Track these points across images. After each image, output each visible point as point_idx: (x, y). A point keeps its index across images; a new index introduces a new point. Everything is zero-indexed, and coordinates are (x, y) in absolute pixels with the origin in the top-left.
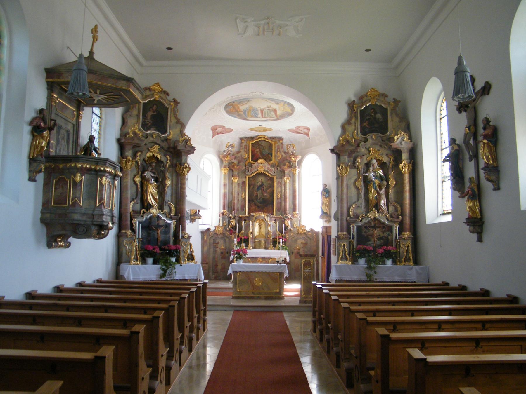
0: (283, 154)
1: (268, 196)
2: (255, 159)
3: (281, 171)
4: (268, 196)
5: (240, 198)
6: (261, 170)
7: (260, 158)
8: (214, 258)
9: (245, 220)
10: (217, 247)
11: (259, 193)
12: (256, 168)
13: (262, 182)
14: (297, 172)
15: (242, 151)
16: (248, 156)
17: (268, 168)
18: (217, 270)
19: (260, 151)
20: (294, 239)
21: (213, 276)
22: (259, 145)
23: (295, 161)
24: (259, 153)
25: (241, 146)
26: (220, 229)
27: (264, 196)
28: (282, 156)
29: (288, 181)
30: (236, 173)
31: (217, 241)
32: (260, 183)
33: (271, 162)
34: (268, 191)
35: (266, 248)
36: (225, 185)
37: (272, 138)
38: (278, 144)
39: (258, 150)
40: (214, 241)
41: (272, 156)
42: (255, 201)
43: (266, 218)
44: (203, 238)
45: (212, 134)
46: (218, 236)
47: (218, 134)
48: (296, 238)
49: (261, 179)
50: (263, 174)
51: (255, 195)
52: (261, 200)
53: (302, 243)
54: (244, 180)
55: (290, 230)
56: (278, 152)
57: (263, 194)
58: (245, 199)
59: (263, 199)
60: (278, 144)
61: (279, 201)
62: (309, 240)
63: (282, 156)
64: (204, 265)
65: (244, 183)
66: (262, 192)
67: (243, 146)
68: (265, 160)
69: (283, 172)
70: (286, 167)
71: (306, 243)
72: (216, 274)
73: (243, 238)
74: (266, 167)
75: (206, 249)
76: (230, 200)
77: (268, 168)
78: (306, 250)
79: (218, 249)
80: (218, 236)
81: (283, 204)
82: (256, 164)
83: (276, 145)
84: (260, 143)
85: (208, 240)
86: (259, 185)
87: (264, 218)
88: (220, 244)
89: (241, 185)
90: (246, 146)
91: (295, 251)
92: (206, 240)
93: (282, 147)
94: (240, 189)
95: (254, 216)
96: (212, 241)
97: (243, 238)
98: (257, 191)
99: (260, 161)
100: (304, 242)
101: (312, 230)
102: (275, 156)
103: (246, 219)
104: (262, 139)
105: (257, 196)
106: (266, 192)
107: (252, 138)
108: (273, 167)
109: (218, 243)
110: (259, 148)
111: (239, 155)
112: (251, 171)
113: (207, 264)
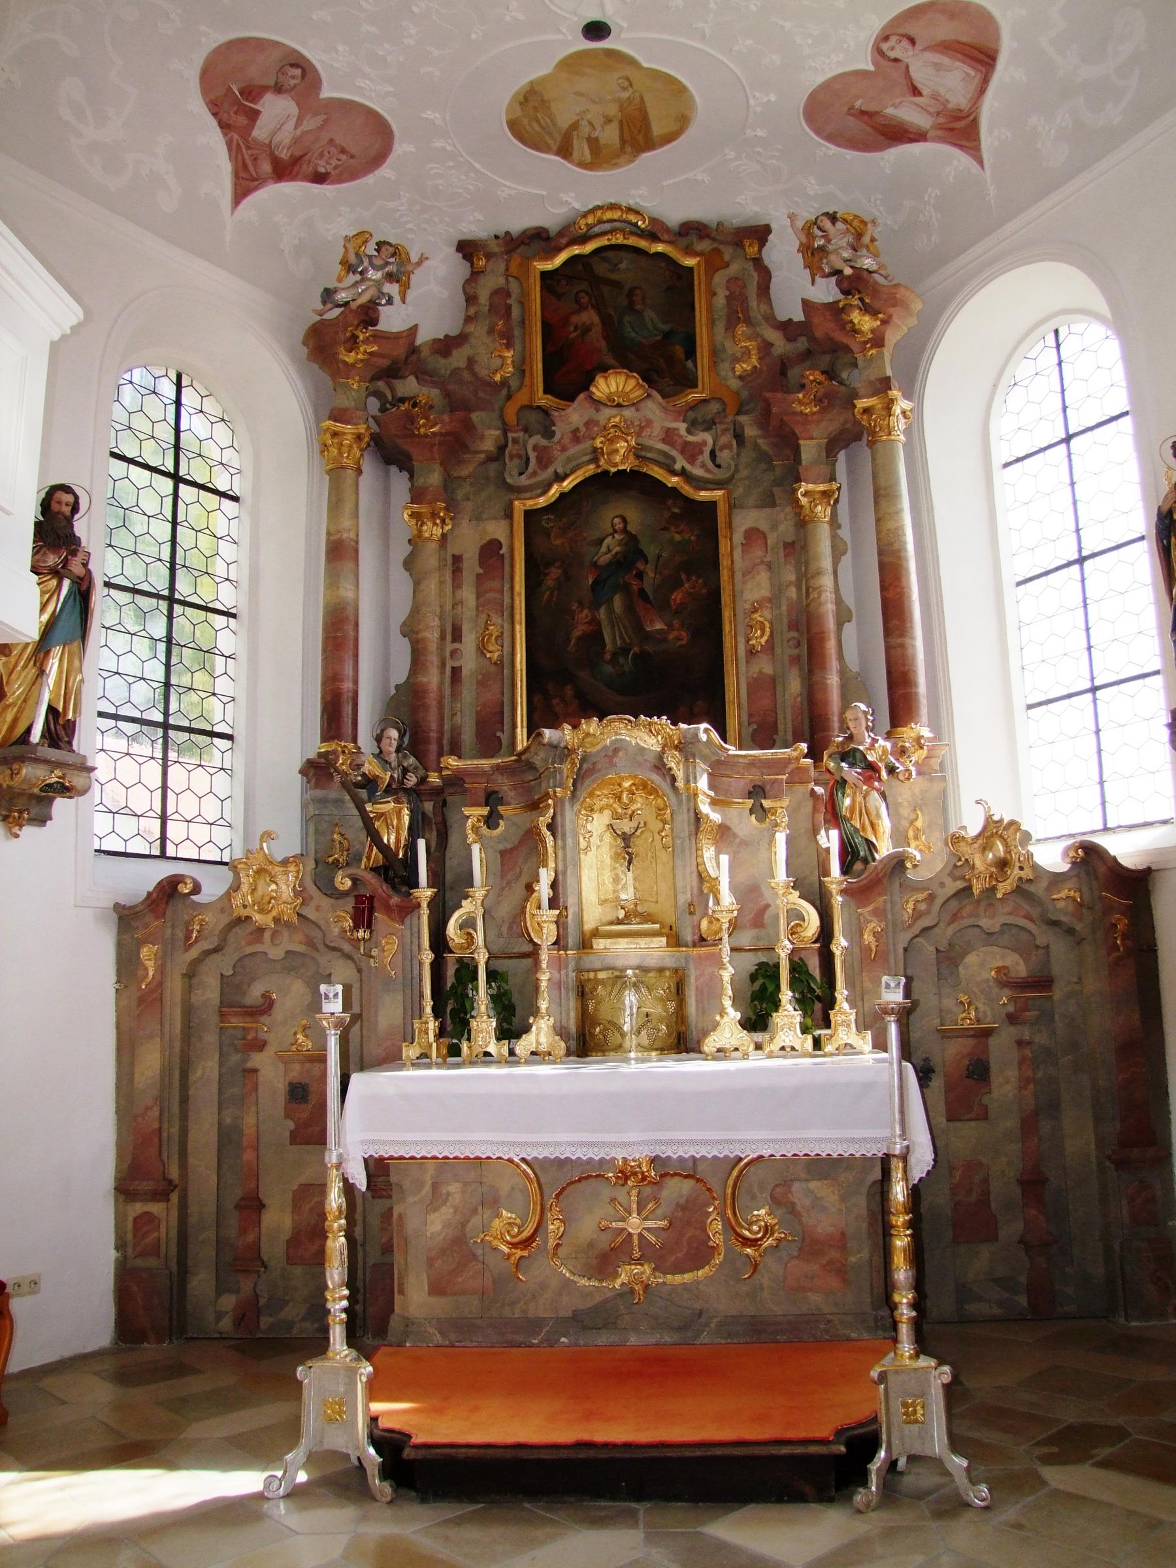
0: (775, 337)
1: (680, 637)
2: (568, 376)
3: (763, 457)
4: (680, 637)
5: (469, 662)
6: (620, 458)
7: (604, 369)
8: (228, 1139)
9: (492, 799)
10: (260, 1045)
11: (610, 620)
12: (576, 437)
13: (631, 540)
14: (899, 424)
15: (478, 331)
16: (522, 370)
17: (669, 436)
18: (256, 1246)
19: (606, 320)
20: (928, 948)
21: (228, 1302)
22: (597, 281)
23: (878, 341)
24: (596, 337)
25: (471, 299)
26: (284, 887)
27: (647, 637)
28: (766, 347)
29: (822, 512)
30: (434, 478)
31: (255, 993)
32: (612, 545)
33: (693, 396)
34: (677, 596)
35: (682, 1041)
36: (340, 552)
37: (692, 231)
38: (734, 268)
39: (590, 317)
40: (231, 987)
41: (691, 353)
42: (584, 675)
43: (673, 761)
44: (127, 965)
45: (225, 166)
46: (266, 946)
47: (283, 171)
48: (945, 934)
49: (622, 517)
50: (631, 483)
51: (577, 633)
52: (627, 663)
53: (1005, 980)
54: (496, 530)
55: (898, 864)
56: (731, 326)
57: (639, 628)
58: (504, 665)
59: (641, 657)
60: (734, 268)
61: (765, 666)
62: (1059, 948)
63: (766, 347)
64: (138, 1208)
65: (491, 552)
66: (630, 609)
67: (484, 297)
68: (649, 378)
69: (788, 442)
70: (803, 405)
71: (1041, 982)
72: (246, 1285)
73: (482, 957)
74: (657, 430)
75: (151, 1061)
76: (400, 673)
77: (669, 436)
78: (1041, 1039)
79: (257, 1060)
80: (266, 946)
81: (794, 685)
82: (575, 415)
83: (720, 278)
84: (601, 269)
85: (175, 987)
86: (604, 559)
87: (660, 766)
88: (278, 1013)
89: (471, 566)
90: (501, 293)
91: (949, 1055)
92: (159, 984)
93: (764, 289)
94: (468, 594)
95: (564, 752)
96: (209, 993)
97: (482, 957)
98: (595, 606)
99: (608, 385)
100: (1020, 968)
101: (1089, 857)
102: (716, 354)
103: (504, 785)
104: (619, 239)
105: (595, 636)
106: (663, 606)
107: (539, 240)
108: (709, 425)
109: (267, 1006)
110: (599, 308)
111: (458, 358)
112: (544, 460)
113: (161, 1195)
